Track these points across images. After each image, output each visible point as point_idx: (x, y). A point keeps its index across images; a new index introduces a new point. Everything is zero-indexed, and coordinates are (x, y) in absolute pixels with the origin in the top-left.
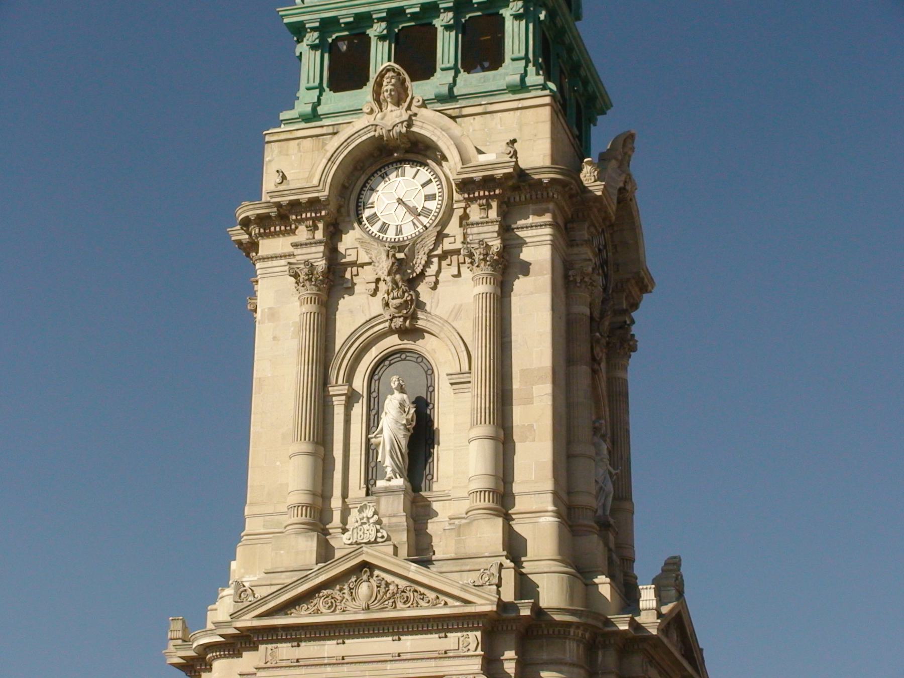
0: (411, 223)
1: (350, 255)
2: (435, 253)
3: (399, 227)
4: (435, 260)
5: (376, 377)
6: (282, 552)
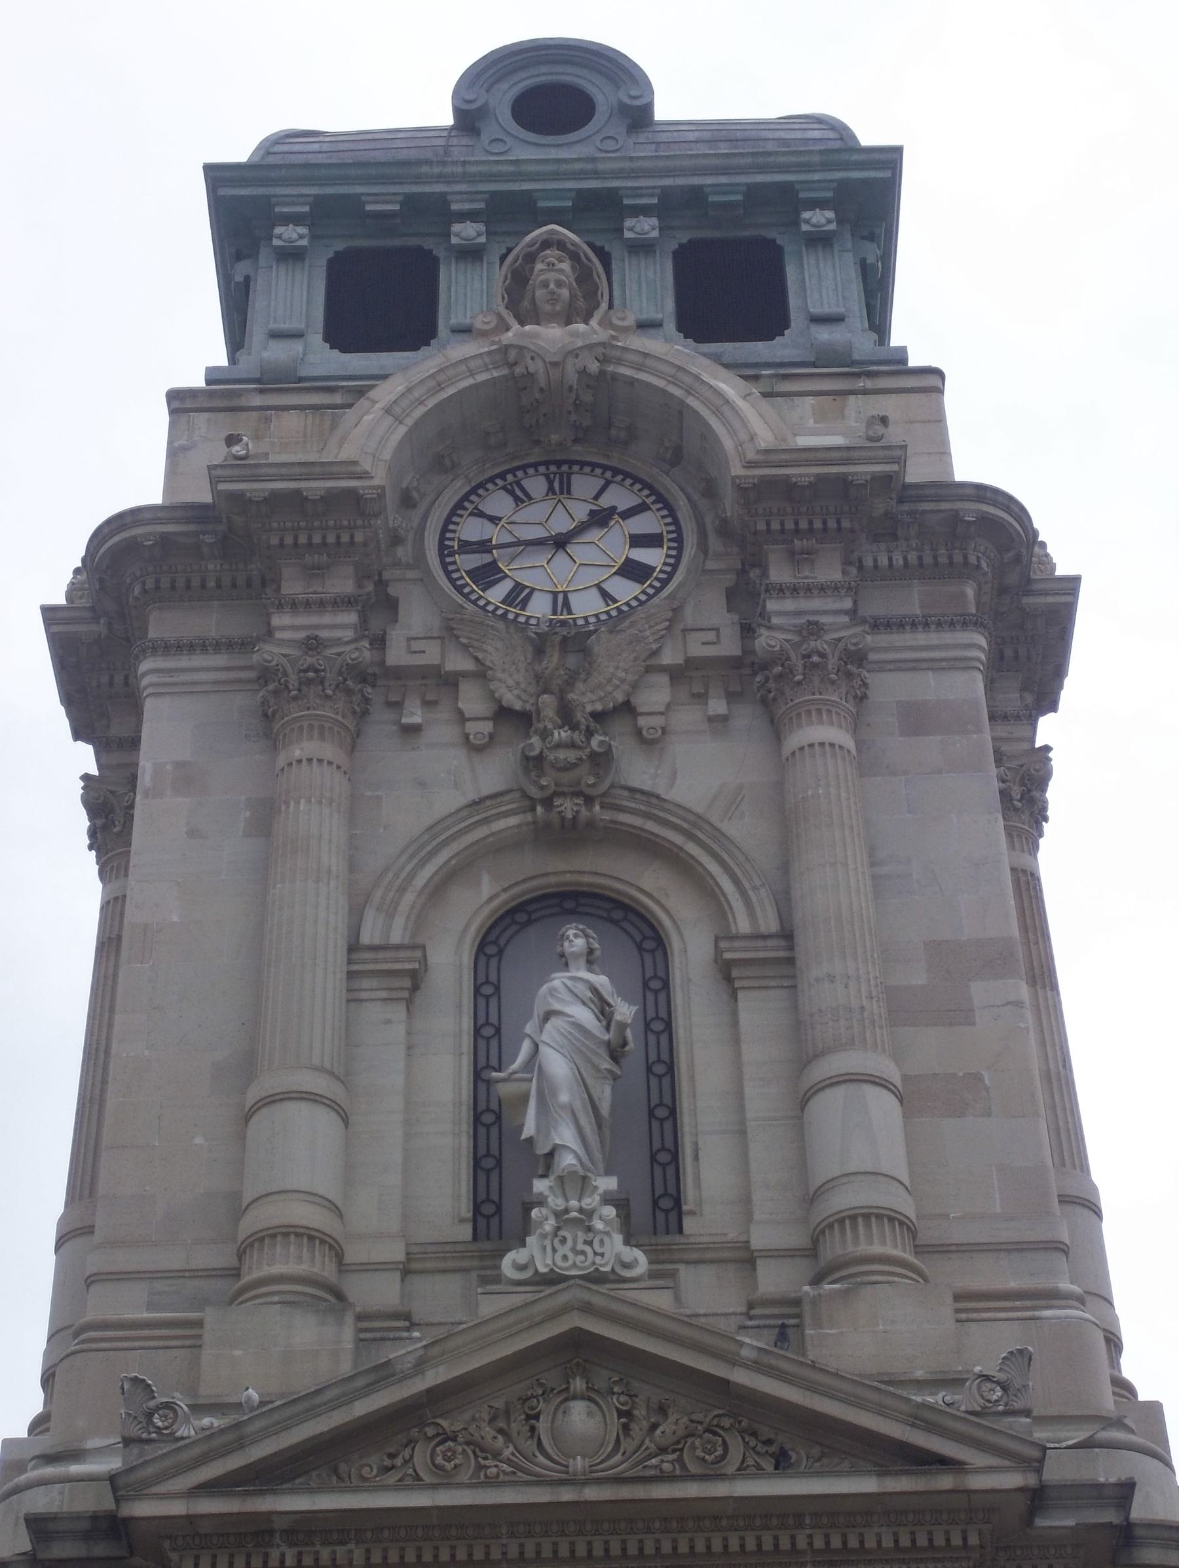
0: (595, 592)
1: (424, 652)
2: (669, 657)
3: (560, 597)
4: (664, 679)
5: (521, 917)
6: (238, 1353)
